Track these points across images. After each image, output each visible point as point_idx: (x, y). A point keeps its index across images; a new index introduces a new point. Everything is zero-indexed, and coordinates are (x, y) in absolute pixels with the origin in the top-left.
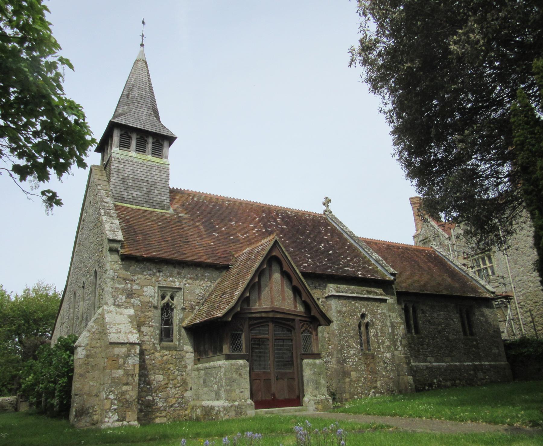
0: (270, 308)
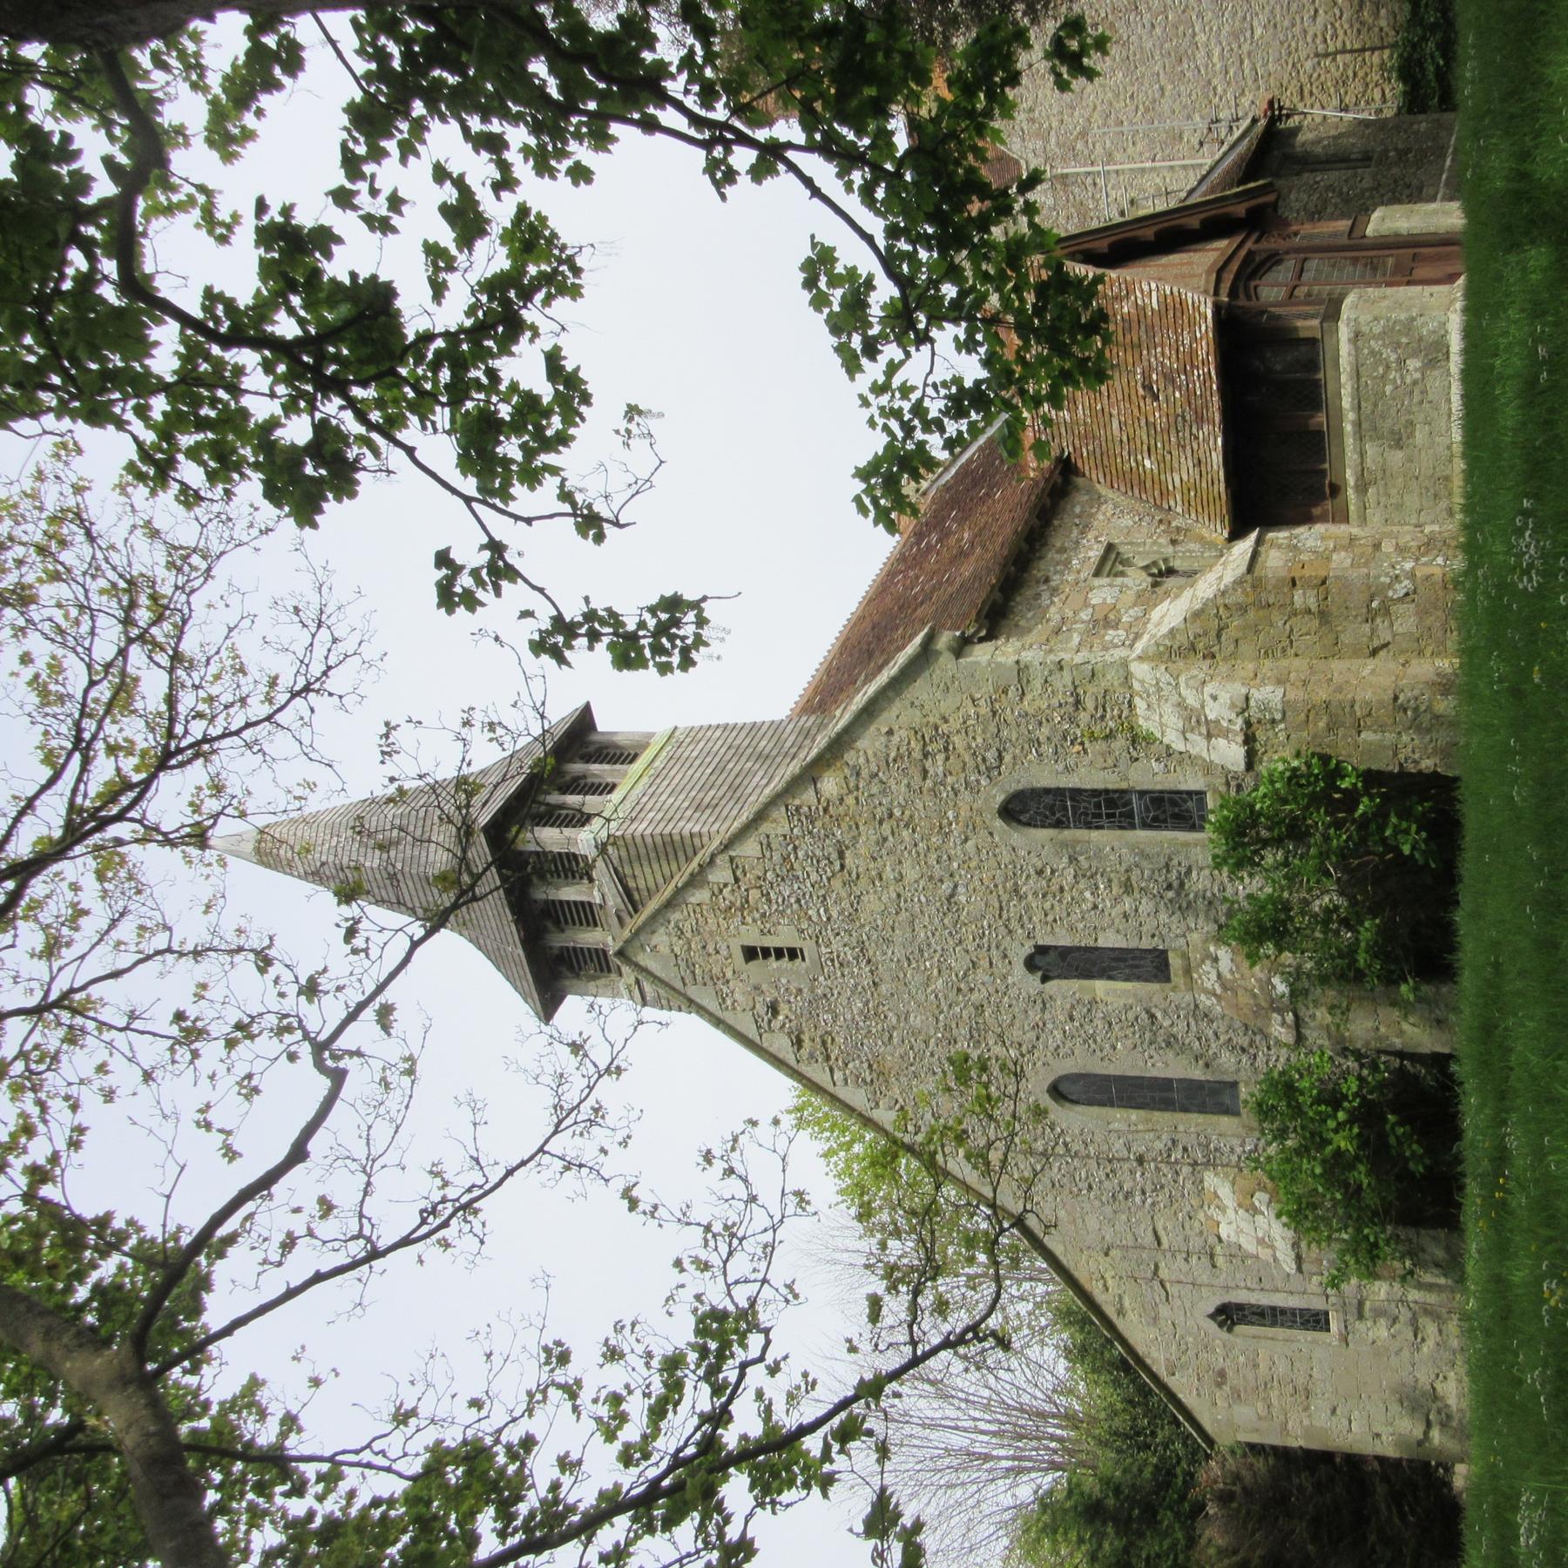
0: (1208, 273)
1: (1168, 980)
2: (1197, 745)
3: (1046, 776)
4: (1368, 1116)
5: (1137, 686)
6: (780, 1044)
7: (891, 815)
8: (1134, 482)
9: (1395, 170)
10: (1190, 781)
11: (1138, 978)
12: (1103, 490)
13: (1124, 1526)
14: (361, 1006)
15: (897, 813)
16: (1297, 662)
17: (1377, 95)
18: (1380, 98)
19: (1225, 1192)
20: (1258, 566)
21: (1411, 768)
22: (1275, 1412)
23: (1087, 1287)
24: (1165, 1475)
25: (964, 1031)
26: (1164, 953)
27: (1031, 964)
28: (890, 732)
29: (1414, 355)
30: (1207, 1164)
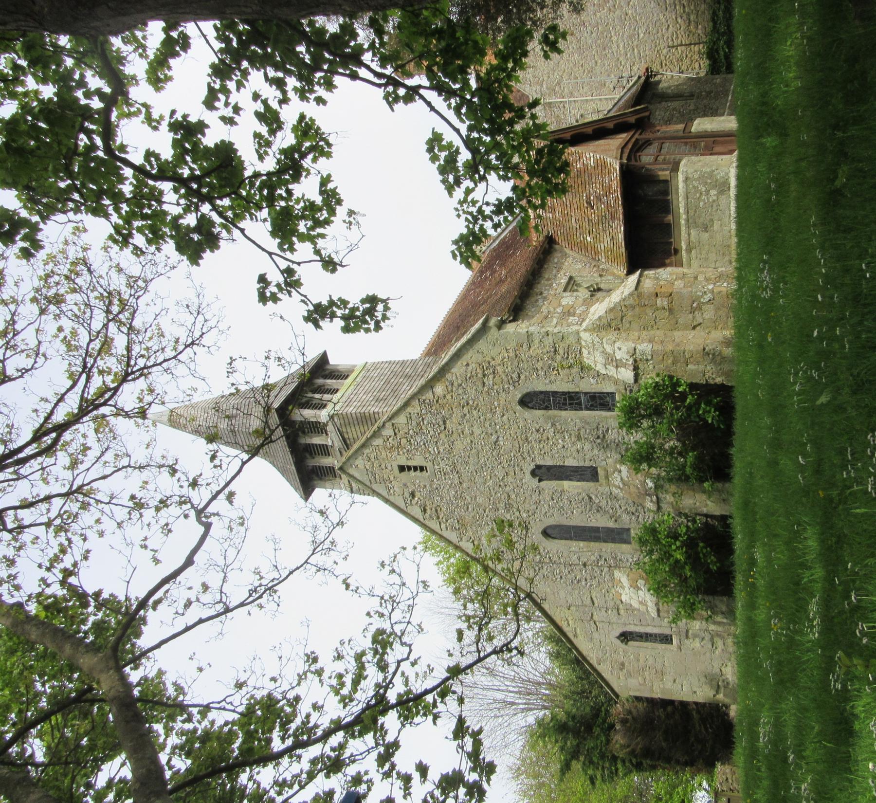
0: (617, 149)
1: (598, 481)
2: (612, 371)
3: (541, 385)
4: (690, 544)
5: (583, 343)
6: (417, 512)
7: (468, 404)
8: (583, 247)
9: (705, 101)
10: (608, 388)
11: (584, 480)
12: (568, 251)
13: (577, 734)
14: (218, 493)
15: (471, 402)
16: (658, 332)
17: (697, 65)
18: (699, 67)
19: (624, 580)
20: (640, 287)
21: (711, 382)
22: (647, 681)
23: (560, 624)
24: (596, 712)
25: (502, 505)
26: (596, 468)
27: (533, 473)
28: (468, 365)
29: (714, 187)
30: (616, 567)
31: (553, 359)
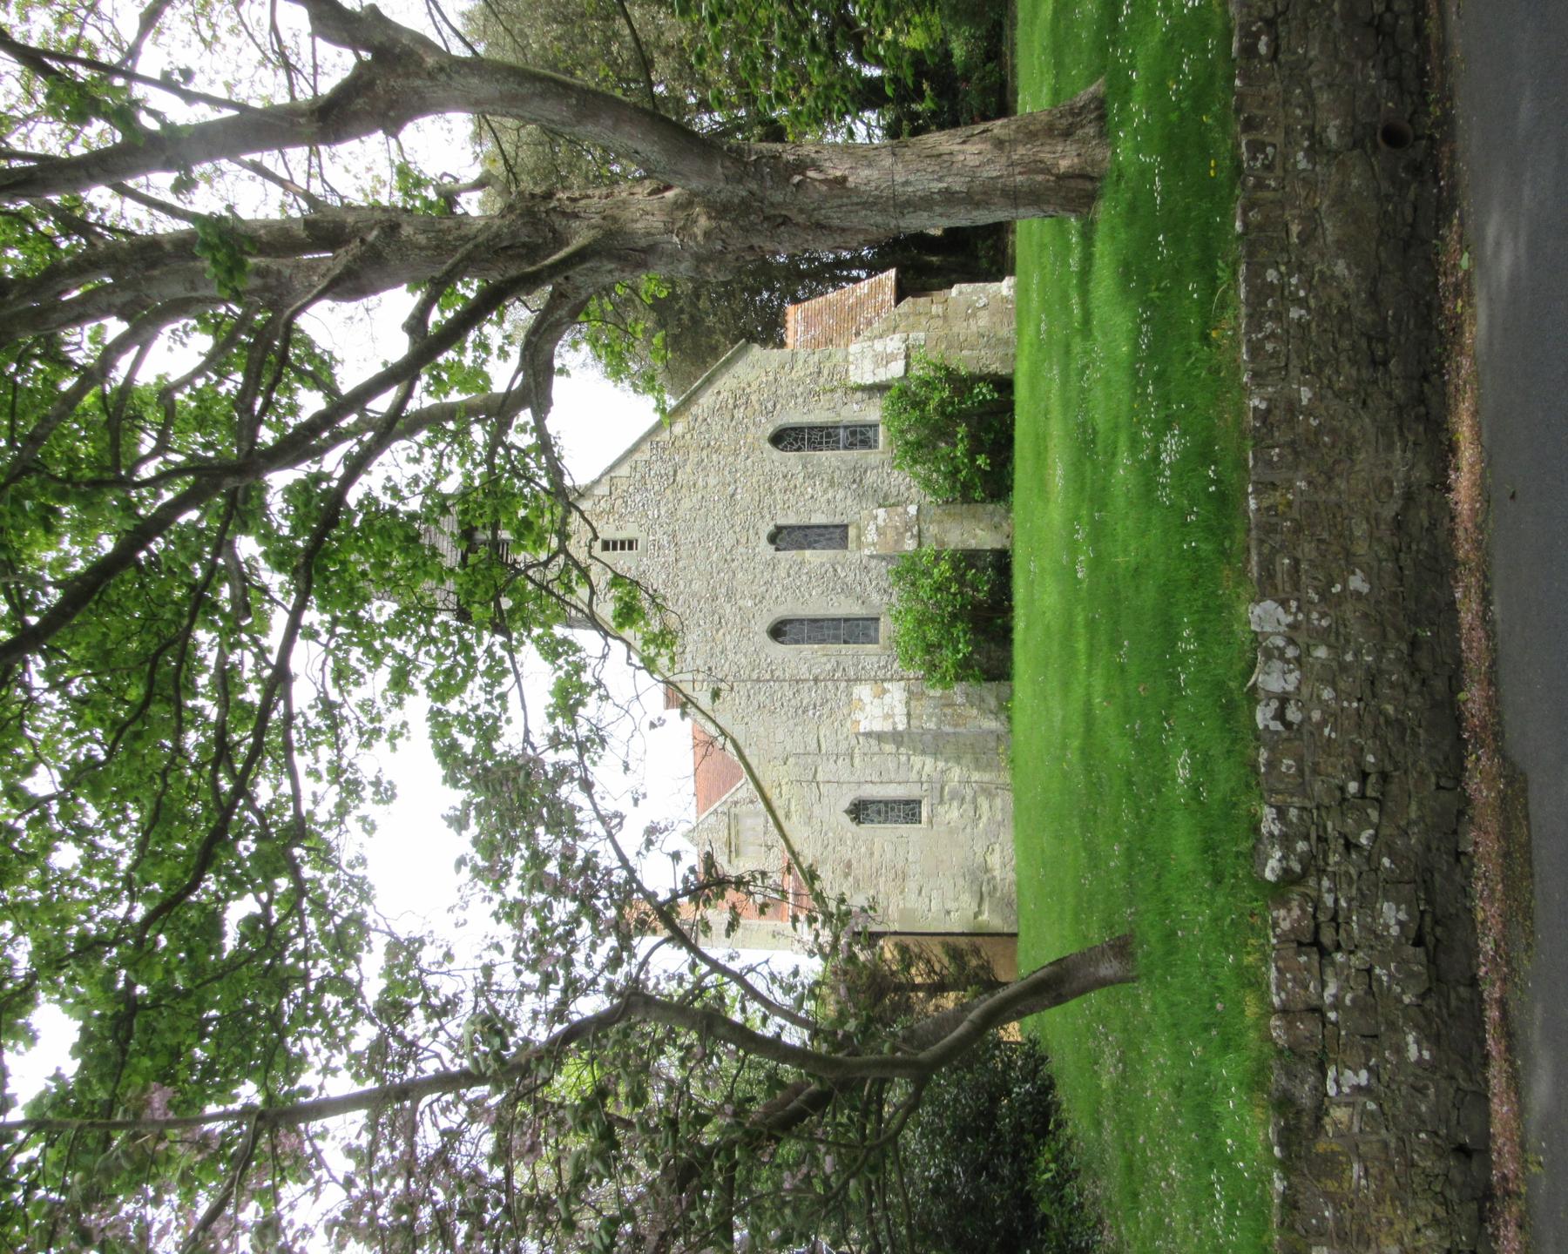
3: (795, 416)
23: (769, 794)
25: (723, 590)
27: (772, 539)
31: (816, 383)
